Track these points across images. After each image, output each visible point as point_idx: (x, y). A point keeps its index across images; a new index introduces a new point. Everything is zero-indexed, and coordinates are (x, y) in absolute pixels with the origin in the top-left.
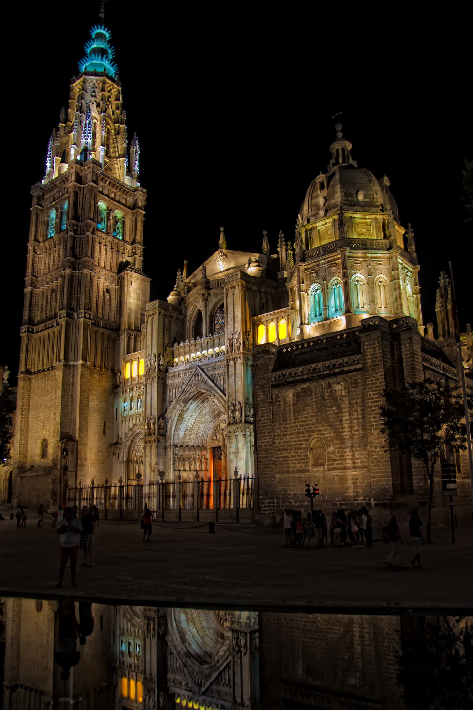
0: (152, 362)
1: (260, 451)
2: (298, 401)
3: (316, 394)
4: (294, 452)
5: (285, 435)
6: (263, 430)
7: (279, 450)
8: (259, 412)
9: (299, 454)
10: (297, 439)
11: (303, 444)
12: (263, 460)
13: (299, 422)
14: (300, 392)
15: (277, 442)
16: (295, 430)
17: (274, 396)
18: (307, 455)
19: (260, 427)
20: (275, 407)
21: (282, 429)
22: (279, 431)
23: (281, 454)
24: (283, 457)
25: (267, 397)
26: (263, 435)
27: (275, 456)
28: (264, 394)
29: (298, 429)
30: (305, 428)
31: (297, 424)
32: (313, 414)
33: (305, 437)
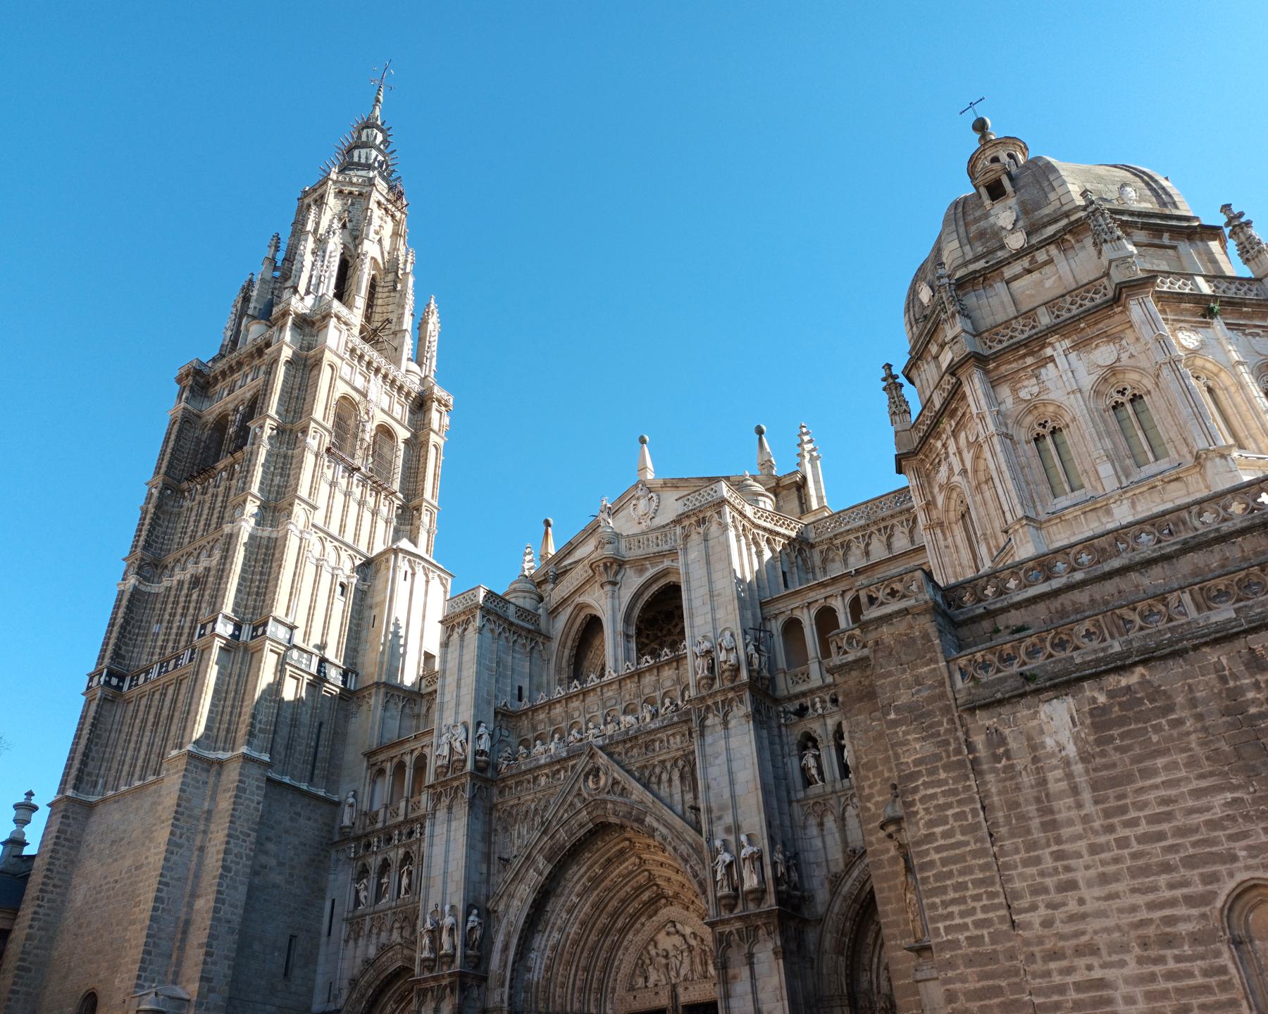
1: (950, 964)
2: (1098, 742)
3: (1193, 703)
4: (1140, 961)
5: (1071, 885)
6: (950, 875)
7: (1055, 955)
8: (919, 807)
9: (1172, 965)
10: (1140, 900)
11: (1188, 919)
13: (1134, 823)
14: (1104, 709)
15: (1035, 918)
16: (1116, 860)
17: (979, 740)
18: (1223, 970)
19: (931, 864)
20: (990, 777)
21: (1048, 863)
22: (1033, 870)
23: (1069, 971)
24: (1078, 987)
25: (947, 743)
26: (952, 895)
27: (1037, 982)
28: (929, 733)
29: (1134, 856)
30: (1173, 849)
31: (1122, 832)
32: (1204, 784)
33: (1185, 883)
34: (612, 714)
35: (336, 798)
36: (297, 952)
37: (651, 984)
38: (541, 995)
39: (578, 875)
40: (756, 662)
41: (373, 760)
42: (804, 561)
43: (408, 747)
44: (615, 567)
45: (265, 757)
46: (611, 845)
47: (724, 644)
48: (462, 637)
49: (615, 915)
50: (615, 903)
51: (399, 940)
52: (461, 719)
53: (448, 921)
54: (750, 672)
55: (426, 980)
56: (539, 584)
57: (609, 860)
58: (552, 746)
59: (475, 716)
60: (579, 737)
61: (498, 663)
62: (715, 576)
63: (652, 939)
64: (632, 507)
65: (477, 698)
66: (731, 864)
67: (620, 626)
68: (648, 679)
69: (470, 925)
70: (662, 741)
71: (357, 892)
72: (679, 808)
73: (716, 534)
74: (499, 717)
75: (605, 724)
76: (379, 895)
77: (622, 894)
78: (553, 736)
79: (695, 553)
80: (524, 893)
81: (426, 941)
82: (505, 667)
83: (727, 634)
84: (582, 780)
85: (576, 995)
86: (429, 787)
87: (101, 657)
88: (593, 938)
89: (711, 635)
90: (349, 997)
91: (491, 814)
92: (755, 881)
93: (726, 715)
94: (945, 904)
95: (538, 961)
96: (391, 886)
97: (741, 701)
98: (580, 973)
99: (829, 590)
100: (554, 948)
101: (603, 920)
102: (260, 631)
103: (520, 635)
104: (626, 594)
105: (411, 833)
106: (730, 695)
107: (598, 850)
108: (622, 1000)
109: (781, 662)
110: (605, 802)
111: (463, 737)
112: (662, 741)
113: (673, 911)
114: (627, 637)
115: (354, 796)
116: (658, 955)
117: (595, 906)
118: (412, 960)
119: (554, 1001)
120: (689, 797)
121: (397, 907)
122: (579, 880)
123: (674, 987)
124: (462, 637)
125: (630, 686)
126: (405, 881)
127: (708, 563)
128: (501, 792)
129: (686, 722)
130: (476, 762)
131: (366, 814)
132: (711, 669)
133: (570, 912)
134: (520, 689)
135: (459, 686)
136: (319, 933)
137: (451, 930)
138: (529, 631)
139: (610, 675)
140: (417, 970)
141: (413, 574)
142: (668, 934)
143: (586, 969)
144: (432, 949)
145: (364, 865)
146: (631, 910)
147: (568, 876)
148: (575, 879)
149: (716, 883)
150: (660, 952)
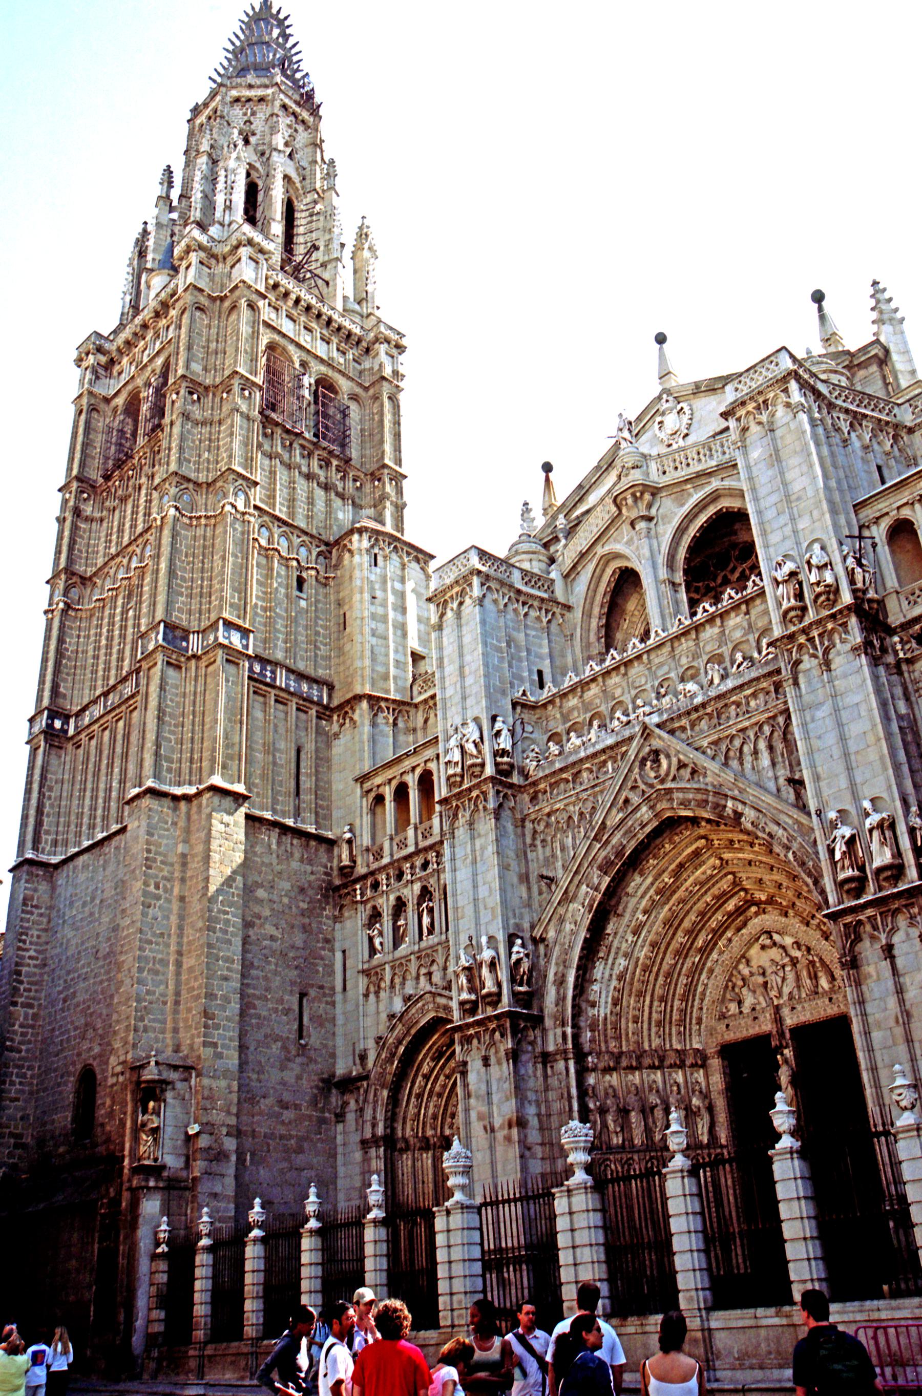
0: (470, 747)
34: (666, 684)
35: (330, 835)
36: (310, 989)
37: (746, 1009)
38: (610, 1033)
39: (640, 886)
40: (859, 577)
41: (367, 785)
43: (407, 764)
44: (647, 496)
45: (240, 788)
46: (684, 845)
47: (814, 561)
48: (458, 615)
49: (692, 933)
50: (692, 917)
51: (428, 988)
52: (470, 714)
53: (487, 954)
54: (854, 592)
55: (468, 1026)
56: (546, 546)
57: (681, 866)
58: (593, 735)
59: (488, 708)
60: (624, 719)
61: (509, 646)
62: (789, 476)
63: (743, 956)
64: (656, 426)
65: (487, 687)
66: (853, 837)
67: (663, 573)
69: (514, 957)
70: (738, 704)
71: (371, 939)
72: (771, 785)
73: (785, 420)
74: (519, 709)
75: (659, 696)
76: (397, 941)
77: (700, 905)
78: (591, 724)
79: (756, 453)
80: (578, 916)
81: (463, 980)
82: (518, 647)
83: (817, 546)
84: (637, 770)
85: (654, 1030)
86: (441, 802)
87: (39, 699)
88: (669, 960)
89: (793, 553)
90: (379, 1055)
91: (523, 827)
92: (888, 854)
93: (826, 652)
96: (410, 927)
97: (847, 632)
98: (656, 1003)
100: (621, 977)
101: (680, 938)
103: (531, 606)
104: (667, 532)
105: (425, 866)
106: (830, 626)
107: (666, 854)
108: (712, 1032)
110: (669, 791)
111: (476, 736)
112: (738, 704)
113: (770, 919)
114: (674, 584)
115: (351, 831)
116: (752, 974)
117: (668, 923)
118: (448, 1009)
119: (627, 1040)
121: (420, 951)
122: (645, 893)
123: (777, 1009)
124: (458, 615)
125: (686, 644)
127: (779, 460)
128: (534, 799)
129: (770, 674)
130: (497, 764)
131: (368, 850)
132: (800, 596)
133: (636, 932)
134: (540, 673)
135: (462, 675)
136: (333, 988)
137: (493, 965)
138: (542, 600)
139: (657, 634)
140: (456, 1015)
141: (385, 557)
142: (763, 947)
143: (663, 999)
144: (472, 990)
145: (374, 907)
146: (713, 924)
147: (630, 890)
148: (639, 893)
149: (834, 864)
150: (754, 970)
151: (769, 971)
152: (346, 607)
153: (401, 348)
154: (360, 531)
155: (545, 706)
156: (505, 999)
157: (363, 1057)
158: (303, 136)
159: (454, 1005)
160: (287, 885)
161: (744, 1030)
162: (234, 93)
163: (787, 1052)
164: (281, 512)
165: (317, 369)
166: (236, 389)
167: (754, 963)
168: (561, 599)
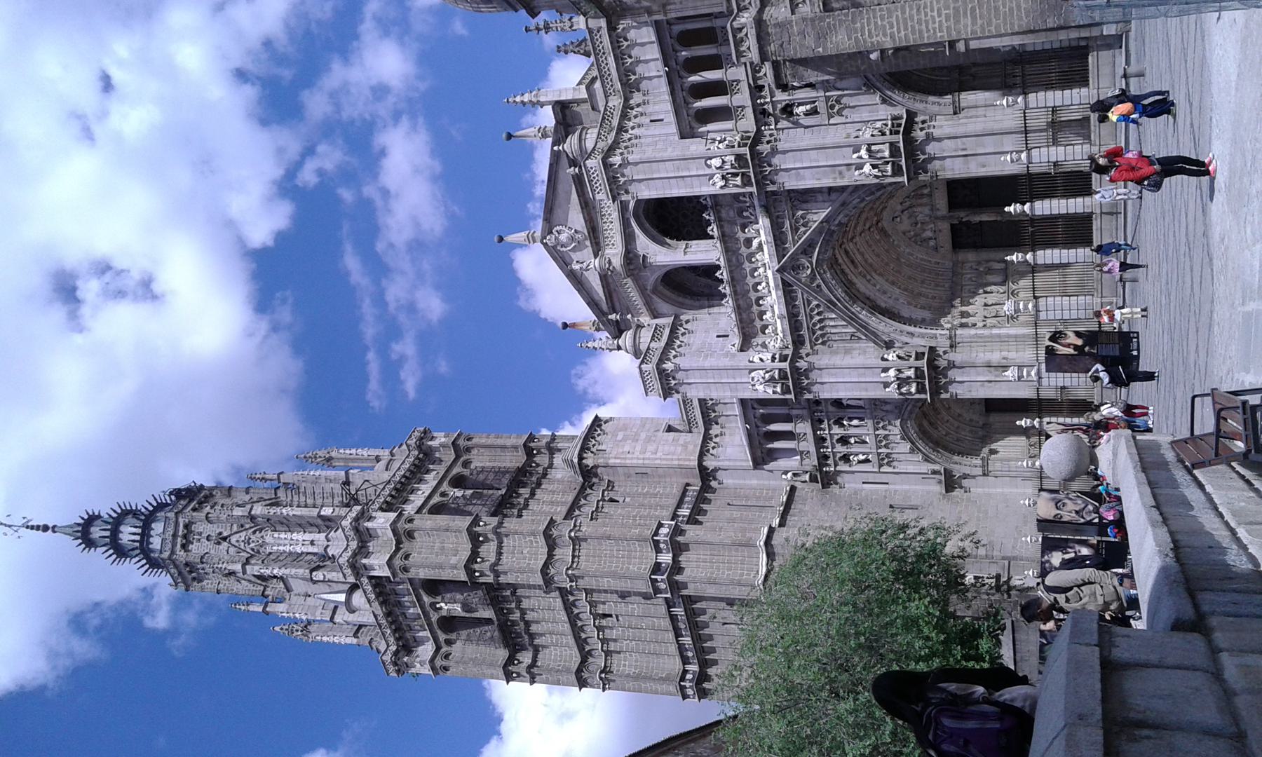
0: (767, 376)
12: (979, 22)
26: (924, 27)
39: (861, 285)
41: (760, 460)
42: (638, 105)
53: (892, 373)
57: (853, 262)
68: (727, 229)
71: (860, 462)
81: (904, 390)
94: (928, 31)
95: (919, 314)
99: (678, 87)
100: (909, 304)
102: (662, 546)
109: (728, 125)
111: (762, 372)
113: (886, 215)
120: (820, 197)
123: (937, 218)
126: (855, 422)
132: (735, 175)
137: (899, 371)
151: (913, 220)
152: (632, 471)
153: (425, 432)
154: (581, 458)
155: (744, 334)
156: (919, 363)
157: (934, 472)
158: (219, 498)
159: (917, 396)
160: (822, 513)
161: (945, 238)
162: (179, 546)
163: (962, 214)
164: (564, 510)
165: (445, 487)
166: (477, 529)
167: (908, 228)
168: (670, 320)
